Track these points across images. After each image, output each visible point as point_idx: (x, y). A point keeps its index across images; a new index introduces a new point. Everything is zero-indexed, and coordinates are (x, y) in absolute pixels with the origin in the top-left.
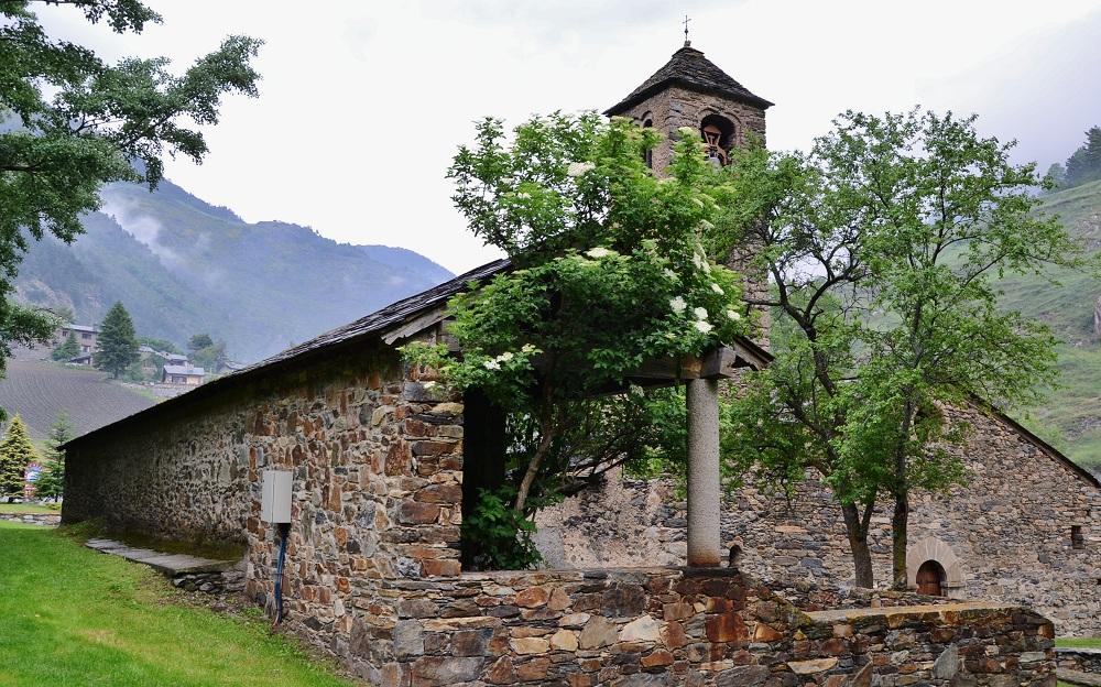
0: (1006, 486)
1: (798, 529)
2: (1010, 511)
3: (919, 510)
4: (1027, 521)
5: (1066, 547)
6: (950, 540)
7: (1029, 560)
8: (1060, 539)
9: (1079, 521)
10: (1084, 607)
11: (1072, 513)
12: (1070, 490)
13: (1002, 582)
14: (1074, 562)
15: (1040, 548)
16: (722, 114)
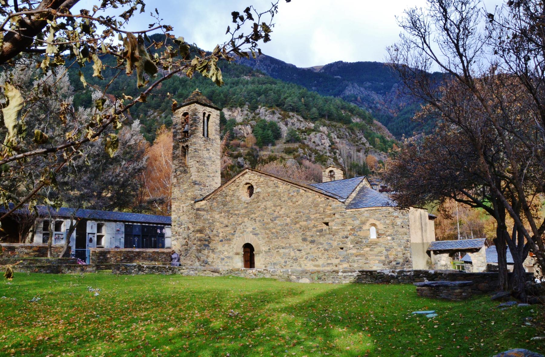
0: (283, 210)
1: (202, 235)
2: (286, 220)
3: (243, 224)
4: (296, 223)
5: (318, 233)
6: (256, 234)
7: (295, 240)
8: (315, 229)
9: (326, 220)
10: (329, 262)
11: (322, 217)
12: (321, 205)
13: (282, 251)
14: (321, 240)
15: (303, 234)
16: (185, 111)
